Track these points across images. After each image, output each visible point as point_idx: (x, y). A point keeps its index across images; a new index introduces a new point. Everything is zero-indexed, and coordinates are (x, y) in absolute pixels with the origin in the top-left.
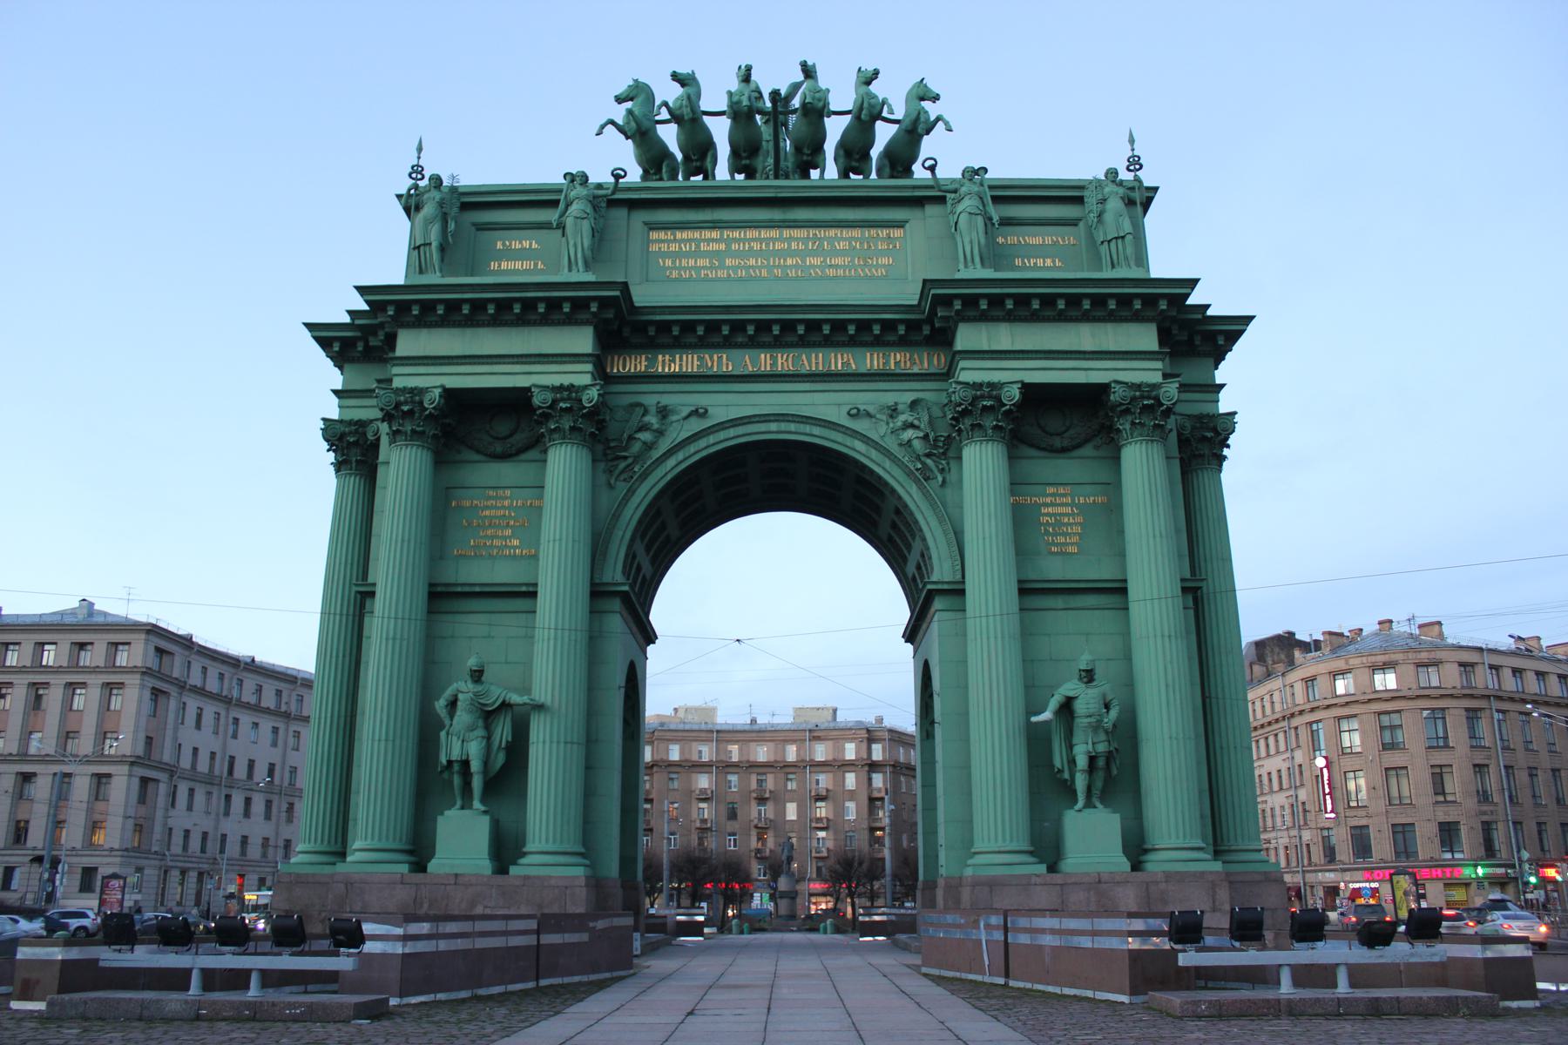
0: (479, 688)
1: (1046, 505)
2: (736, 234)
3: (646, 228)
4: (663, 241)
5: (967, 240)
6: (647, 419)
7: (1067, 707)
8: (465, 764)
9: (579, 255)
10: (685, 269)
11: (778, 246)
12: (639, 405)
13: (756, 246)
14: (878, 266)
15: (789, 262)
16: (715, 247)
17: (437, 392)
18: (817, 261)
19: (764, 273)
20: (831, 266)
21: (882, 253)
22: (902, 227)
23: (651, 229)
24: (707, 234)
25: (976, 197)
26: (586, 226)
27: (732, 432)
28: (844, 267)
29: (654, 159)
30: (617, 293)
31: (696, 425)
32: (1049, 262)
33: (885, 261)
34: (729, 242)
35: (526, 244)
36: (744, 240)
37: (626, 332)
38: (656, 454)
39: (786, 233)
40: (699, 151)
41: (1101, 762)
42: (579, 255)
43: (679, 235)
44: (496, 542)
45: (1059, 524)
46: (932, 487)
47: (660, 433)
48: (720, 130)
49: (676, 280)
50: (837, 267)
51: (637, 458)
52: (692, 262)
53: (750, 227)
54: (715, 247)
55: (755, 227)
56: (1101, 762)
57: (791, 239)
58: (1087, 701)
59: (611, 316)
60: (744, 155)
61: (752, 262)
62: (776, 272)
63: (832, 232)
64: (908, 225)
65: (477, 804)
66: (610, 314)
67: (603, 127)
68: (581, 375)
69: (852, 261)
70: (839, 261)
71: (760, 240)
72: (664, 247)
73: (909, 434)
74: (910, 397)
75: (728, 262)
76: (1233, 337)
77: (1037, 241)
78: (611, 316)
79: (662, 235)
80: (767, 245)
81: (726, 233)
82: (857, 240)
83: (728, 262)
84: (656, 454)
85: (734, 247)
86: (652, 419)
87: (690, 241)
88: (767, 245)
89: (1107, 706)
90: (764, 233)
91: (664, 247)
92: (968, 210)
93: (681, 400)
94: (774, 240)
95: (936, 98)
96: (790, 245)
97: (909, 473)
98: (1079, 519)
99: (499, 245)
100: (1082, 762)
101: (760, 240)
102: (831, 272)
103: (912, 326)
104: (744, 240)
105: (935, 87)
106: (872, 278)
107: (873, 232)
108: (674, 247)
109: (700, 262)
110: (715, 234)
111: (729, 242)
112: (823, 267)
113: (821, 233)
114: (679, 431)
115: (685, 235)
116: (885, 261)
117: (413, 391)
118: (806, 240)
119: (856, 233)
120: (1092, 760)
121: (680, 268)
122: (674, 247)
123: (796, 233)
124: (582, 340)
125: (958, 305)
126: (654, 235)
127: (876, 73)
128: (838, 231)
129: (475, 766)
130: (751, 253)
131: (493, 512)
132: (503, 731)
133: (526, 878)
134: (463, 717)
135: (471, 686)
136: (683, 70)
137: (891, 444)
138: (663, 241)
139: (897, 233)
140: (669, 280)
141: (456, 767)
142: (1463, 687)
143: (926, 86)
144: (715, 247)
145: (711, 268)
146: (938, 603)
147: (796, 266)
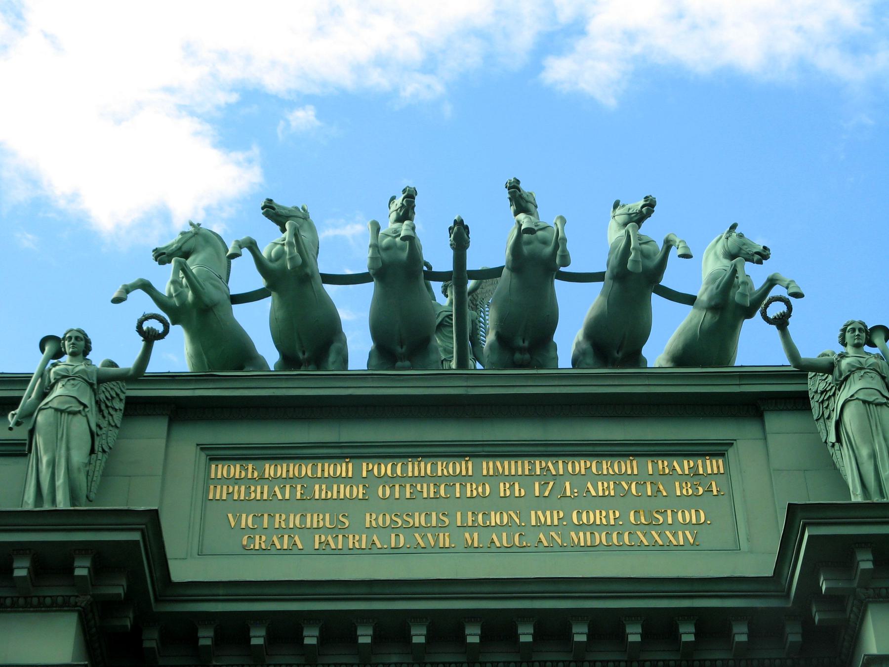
2: (386, 468)
3: (203, 456)
4: (237, 481)
5: (864, 452)
9: (60, 481)
10: (280, 532)
13: (427, 490)
14: (674, 527)
18: (550, 517)
19: (445, 540)
20: (581, 526)
22: (722, 455)
23: (213, 459)
24: (328, 468)
25: (874, 374)
26: (79, 427)
28: (608, 528)
30: (136, 536)
33: (691, 516)
34: (370, 482)
37: (151, 640)
39: (488, 466)
42: (60, 481)
43: (269, 469)
49: (262, 552)
50: (592, 527)
52: (295, 520)
53: (414, 456)
54: (344, 491)
55: (425, 456)
59: (120, 591)
60: (400, 350)
61: (419, 519)
63: (580, 465)
64: (731, 452)
66: (118, 588)
67: (128, 290)
69: (624, 516)
70: (597, 517)
71: (435, 479)
72: (240, 492)
78: (120, 591)
79: (235, 470)
80: (450, 487)
82: (629, 477)
88: (450, 487)
90: (443, 467)
91: (240, 492)
92: (861, 396)
94: (464, 479)
95: (762, 256)
96: (495, 489)
101: (435, 479)
102: (583, 538)
107: (663, 464)
108: (259, 492)
110: (344, 469)
111: (370, 482)
112: (565, 525)
113: (558, 466)
115: (282, 469)
116: (691, 516)
119: (630, 466)
122: (259, 492)
123: (508, 466)
126: (220, 470)
138: (237, 481)
143: (741, 236)
144: (344, 491)
145: (336, 529)
147: (509, 526)
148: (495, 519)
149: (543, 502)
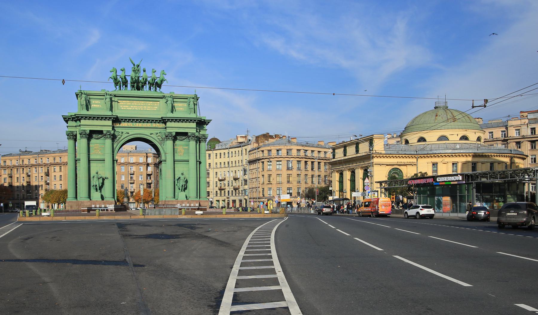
0: (97, 175)
1: (179, 148)
2: (132, 102)
6: (119, 134)
7: (179, 178)
8: (96, 185)
11: (139, 104)
12: (118, 131)
15: (141, 107)
16: (129, 104)
17: (88, 131)
18: (145, 107)
21: (156, 106)
24: (128, 101)
27: (132, 136)
29: (116, 83)
31: (127, 135)
32: (182, 109)
33: (156, 107)
35: (98, 102)
36: (134, 103)
38: (121, 139)
40: (125, 83)
41: (184, 186)
44: (97, 152)
45: (180, 151)
46: (162, 145)
47: (121, 136)
48: (129, 79)
51: (118, 140)
52: (125, 106)
56: (184, 186)
57: (141, 103)
58: (182, 177)
62: (139, 109)
63: (148, 102)
65: (98, 191)
68: (110, 129)
70: (149, 107)
73: (159, 137)
74: (159, 131)
75: (131, 107)
76: (209, 122)
77: (180, 105)
81: (131, 101)
83: (131, 107)
84: (121, 139)
85: (132, 104)
86: (120, 134)
87: (125, 103)
89: (185, 178)
90: (137, 102)
93: (125, 131)
97: (159, 143)
98: (183, 150)
99: (93, 102)
100: (181, 186)
101: (136, 103)
102: (148, 109)
103: (160, 121)
104: (134, 103)
105: (166, 73)
106: (154, 110)
109: (127, 106)
110: (129, 102)
113: (146, 102)
114: (125, 135)
116: (156, 107)
117: (84, 130)
118: (143, 103)
119: (152, 102)
120: (182, 185)
121: (123, 107)
122: (122, 104)
124: (110, 123)
125: (167, 120)
127: (155, 72)
128: (149, 102)
129: (98, 186)
130: (135, 105)
131: (96, 147)
132: (101, 181)
133: (107, 201)
134: (95, 179)
135: (96, 175)
136: (123, 69)
137: (156, 138)
139: (158, 103)
140: (122, 109)
141: (95, 186)
142: (297, 156)
144: (129, 104)
146: (163, 162)
148: (141, 107)
149: (145, 106)
